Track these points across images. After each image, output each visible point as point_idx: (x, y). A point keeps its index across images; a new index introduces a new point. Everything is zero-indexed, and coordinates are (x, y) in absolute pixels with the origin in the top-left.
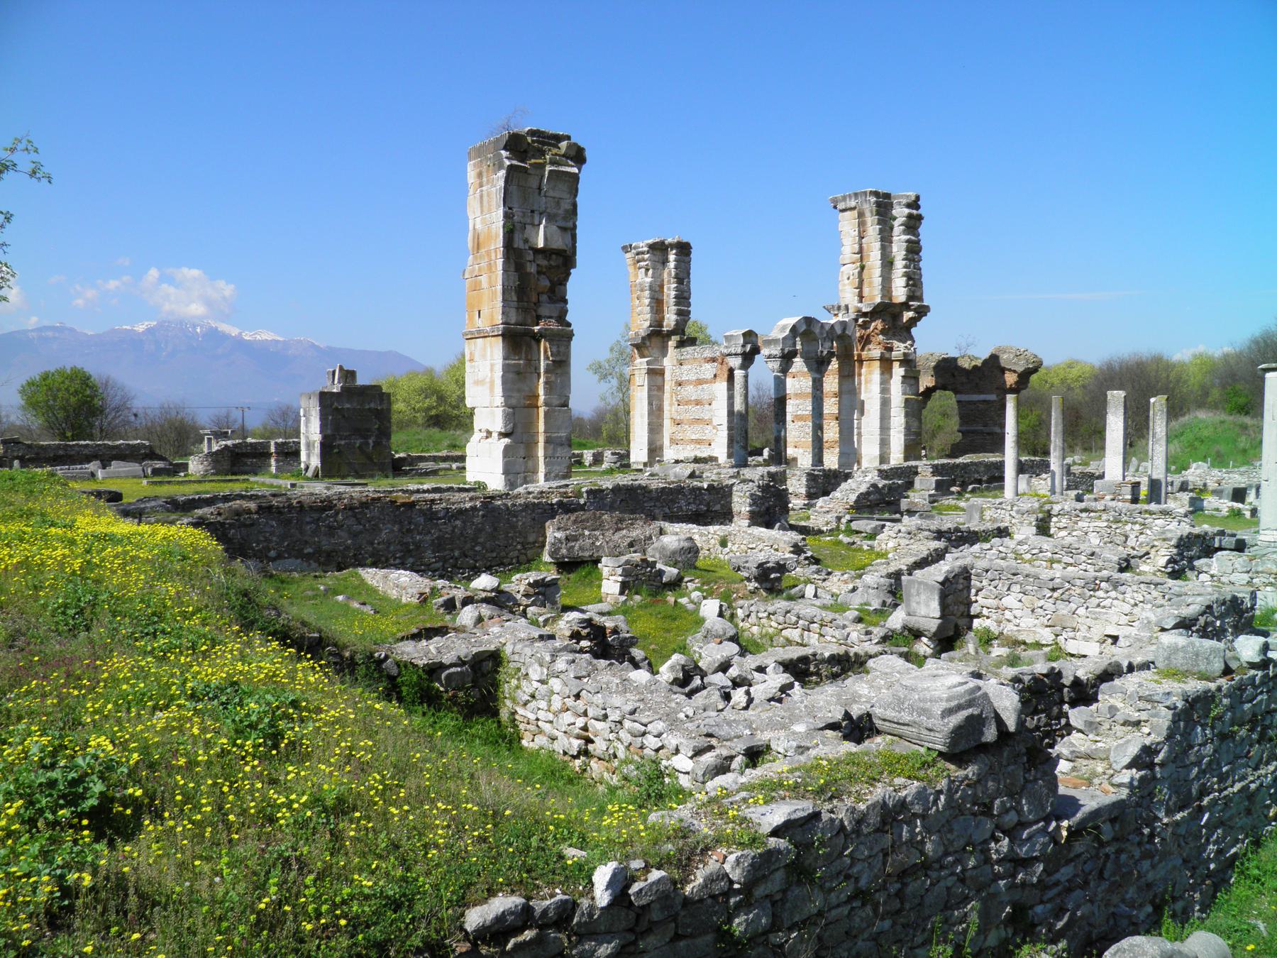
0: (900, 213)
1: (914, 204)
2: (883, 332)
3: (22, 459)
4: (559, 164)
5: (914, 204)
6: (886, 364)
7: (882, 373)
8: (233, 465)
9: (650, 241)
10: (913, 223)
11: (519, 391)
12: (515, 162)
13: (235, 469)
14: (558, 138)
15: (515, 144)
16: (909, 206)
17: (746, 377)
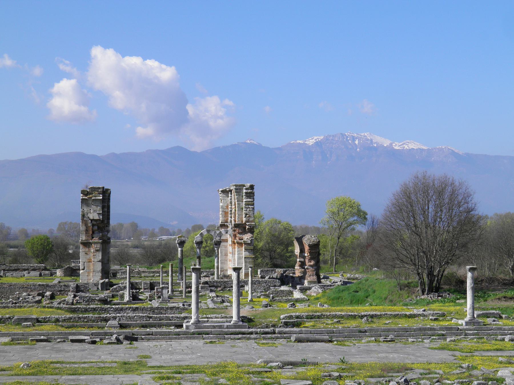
0: (244, 191)
1: (252, 187)
2: (239, 233)
3: (4, 270)
4: (96, 196)
5: (252, 187)
6: (240, 244)
7: (239, 248)
8: (72, 273)
9: (221, 190)
10: (250, 195)
11: (86, 258)
12: (84, 197)
13: (73, 274)
14: (99, 188)
15: (84, 193)
16: (246, 189)
17: (182, 251)
